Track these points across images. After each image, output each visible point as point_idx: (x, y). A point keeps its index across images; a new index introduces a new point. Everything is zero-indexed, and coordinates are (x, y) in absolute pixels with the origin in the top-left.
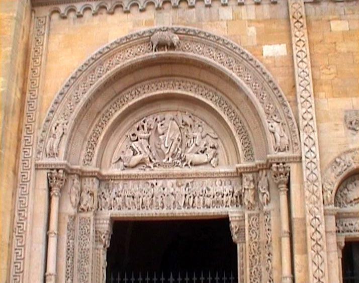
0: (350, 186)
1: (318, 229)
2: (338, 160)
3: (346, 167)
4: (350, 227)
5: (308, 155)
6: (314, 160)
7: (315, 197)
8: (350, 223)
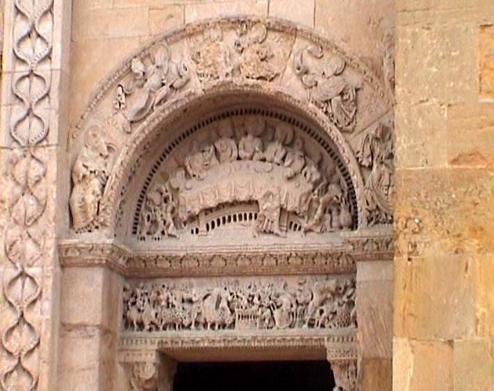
0: (196, 161)
1: (28, 317)
2: (138, 67)
3: (165, 90)
4: (179, 312)
5: (26, 50)
6: (44, 69)
7: (31, 201)
8: (186, 296)
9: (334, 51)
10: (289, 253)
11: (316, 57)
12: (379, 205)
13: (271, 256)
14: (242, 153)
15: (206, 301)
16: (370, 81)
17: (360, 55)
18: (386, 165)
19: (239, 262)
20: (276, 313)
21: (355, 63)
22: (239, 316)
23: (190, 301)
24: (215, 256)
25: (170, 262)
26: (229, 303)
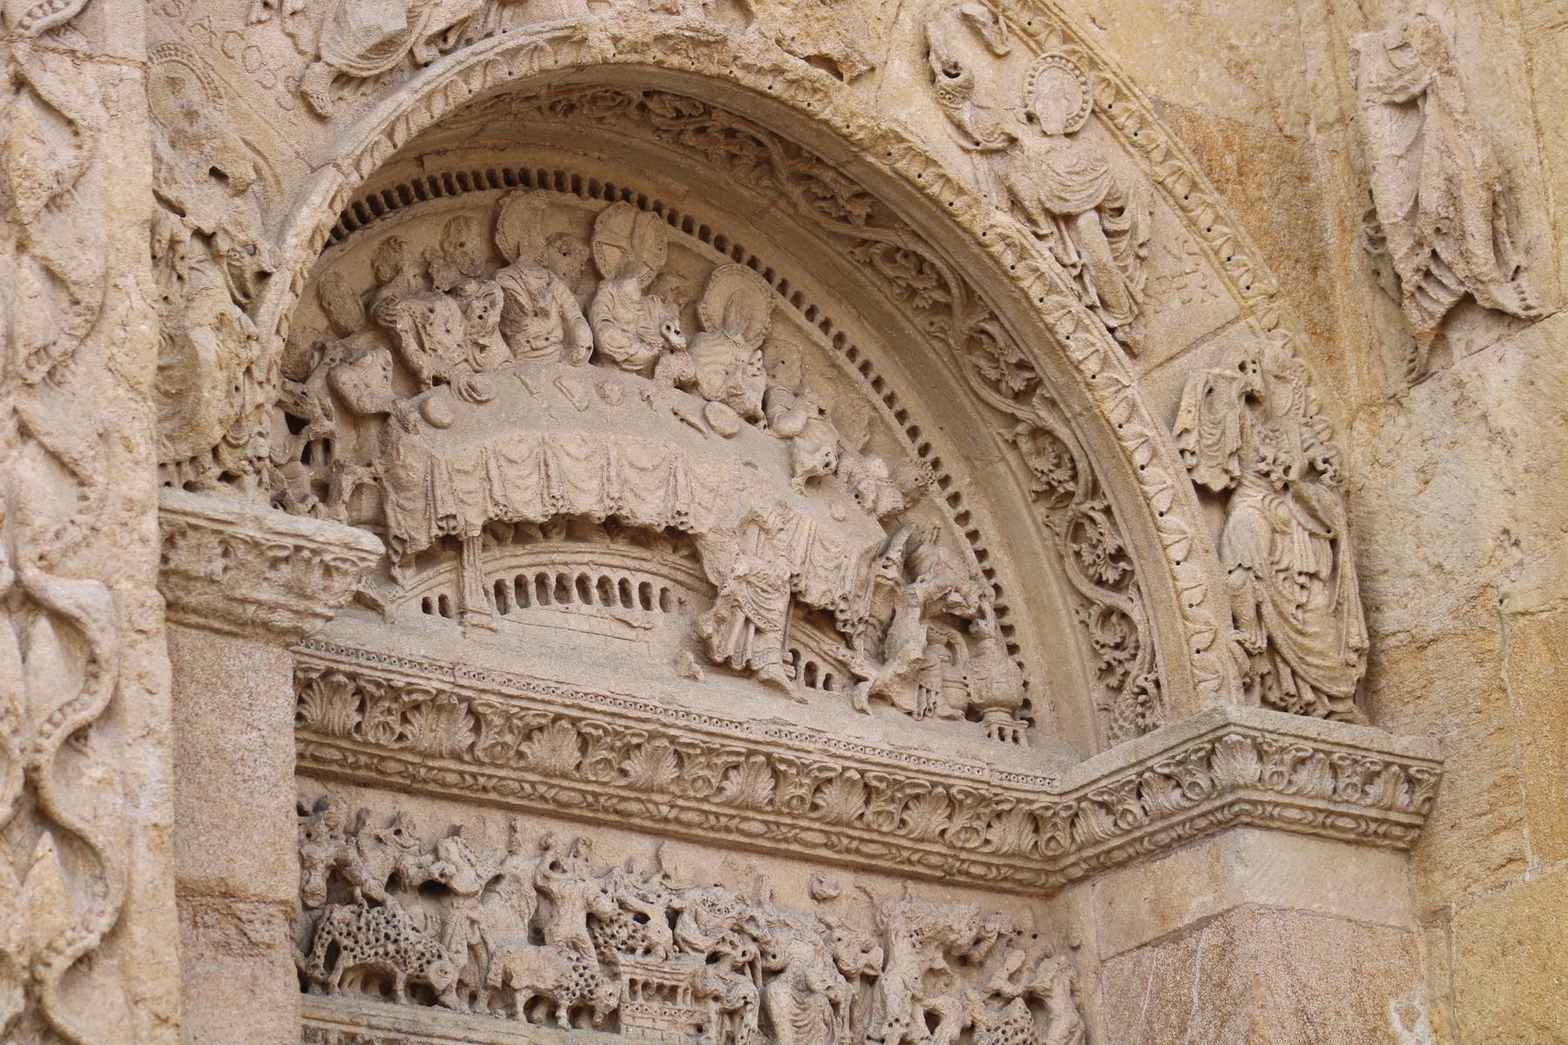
8: (413, 869)
9: (1054, 45)
10: (838, 765)
11: (988, 47)
12: (1279, 639)
13: (770, 761)
14: (613, 340)
15: (495, 901)
16: (1181, 190)
17: (1152, 90)
18: (1299, 499)
19: (635, 766)
20: (781, 995)
21: (1131, 114)
22: (633, 982)
23: (436, 889)
24: (558, 718)
25: (361, 709)
26: (592, 918)
